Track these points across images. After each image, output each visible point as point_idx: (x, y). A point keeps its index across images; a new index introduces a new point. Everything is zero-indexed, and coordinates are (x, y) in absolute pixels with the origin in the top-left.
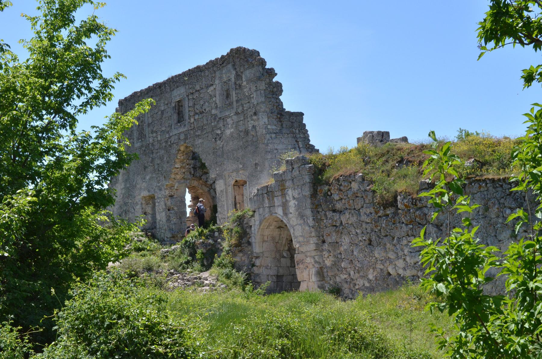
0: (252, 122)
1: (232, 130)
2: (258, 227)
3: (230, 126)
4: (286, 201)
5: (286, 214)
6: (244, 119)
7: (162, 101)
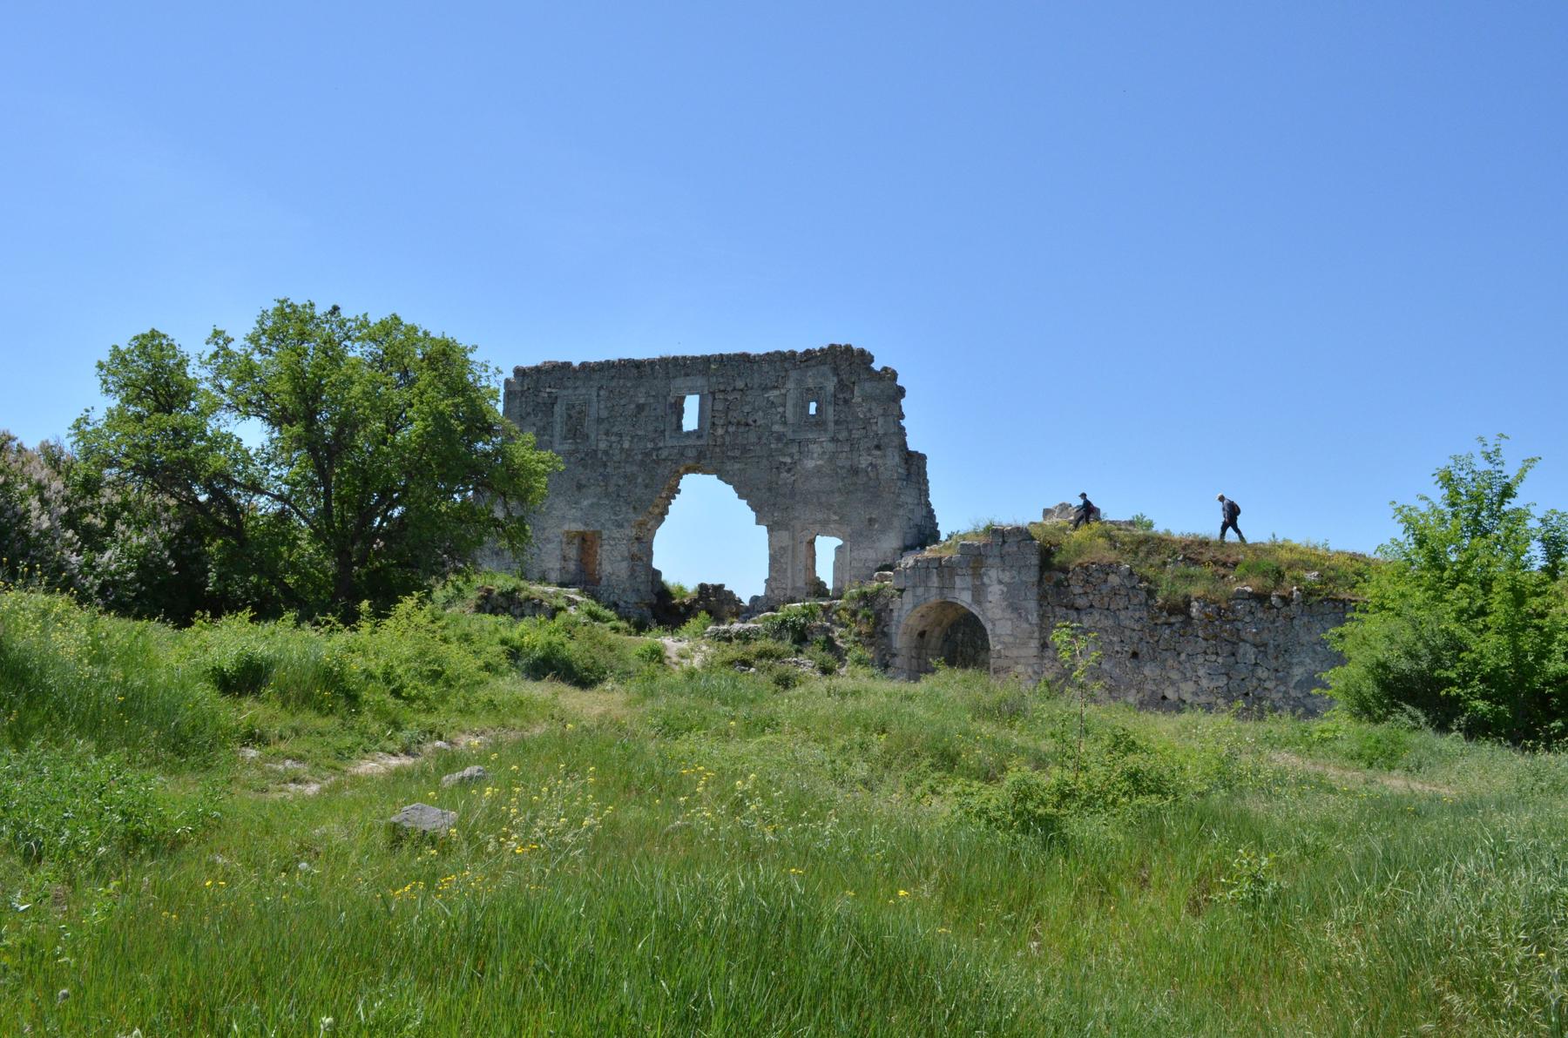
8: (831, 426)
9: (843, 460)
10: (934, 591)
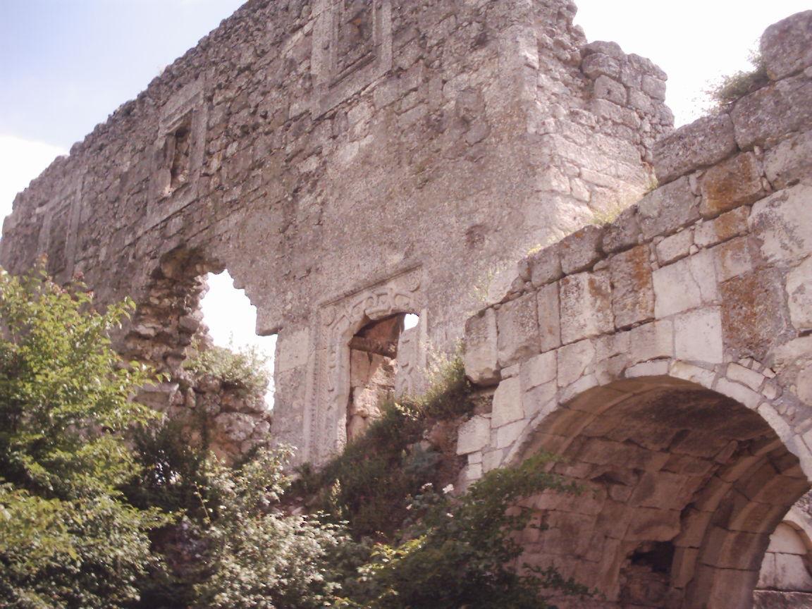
0: (465, 76)
3: (358, 129)
5: (746, 344)
6: (426, 80)
7: (128, 148)
8: (386, 49)
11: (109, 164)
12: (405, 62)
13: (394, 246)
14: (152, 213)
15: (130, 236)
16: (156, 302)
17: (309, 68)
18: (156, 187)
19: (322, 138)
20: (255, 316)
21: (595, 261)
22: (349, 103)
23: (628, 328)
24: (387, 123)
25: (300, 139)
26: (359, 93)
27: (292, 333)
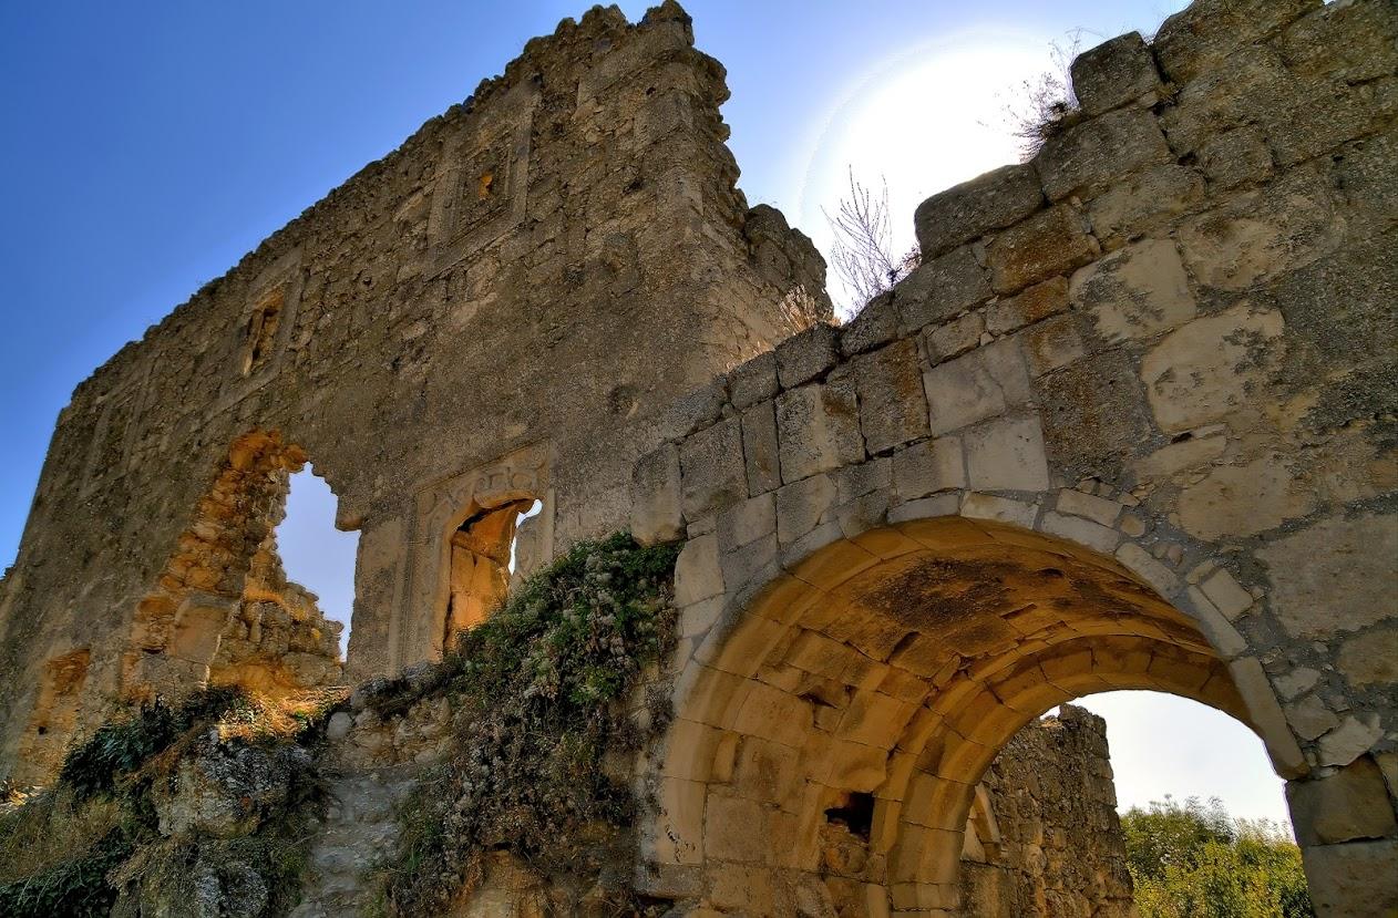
0: (614, 223)
1: (492, 297)
2: (706, 649)
4: (1099, 348)
5: (1088, 463)
6: (567, 229)
8: (521, 200)
9: (548, 266)
10: (823, 497)
11: (182, 346)
12: (540, 214)
13: (516, 417)
14: (226, 394)
15: (198, 421)
16: (219, 497)
17: (426, 229)
18: (234, 366)
19: (435, 302)
20: (335, 506)
21: (828, 370)
22: (470, 261)
23: (889, 453)
24: (515, 278)
25: (407, 303)
26: (482, 250)
27: (380, 523)
